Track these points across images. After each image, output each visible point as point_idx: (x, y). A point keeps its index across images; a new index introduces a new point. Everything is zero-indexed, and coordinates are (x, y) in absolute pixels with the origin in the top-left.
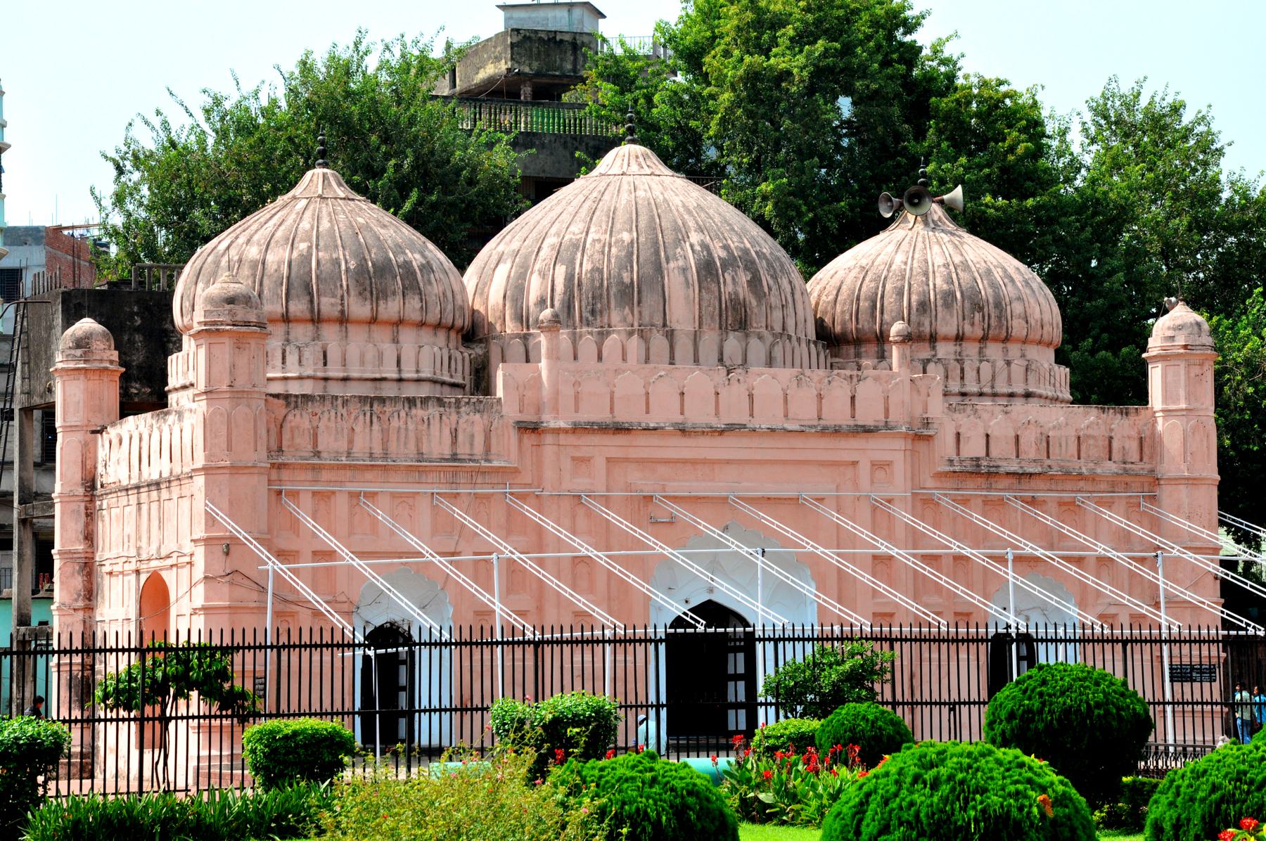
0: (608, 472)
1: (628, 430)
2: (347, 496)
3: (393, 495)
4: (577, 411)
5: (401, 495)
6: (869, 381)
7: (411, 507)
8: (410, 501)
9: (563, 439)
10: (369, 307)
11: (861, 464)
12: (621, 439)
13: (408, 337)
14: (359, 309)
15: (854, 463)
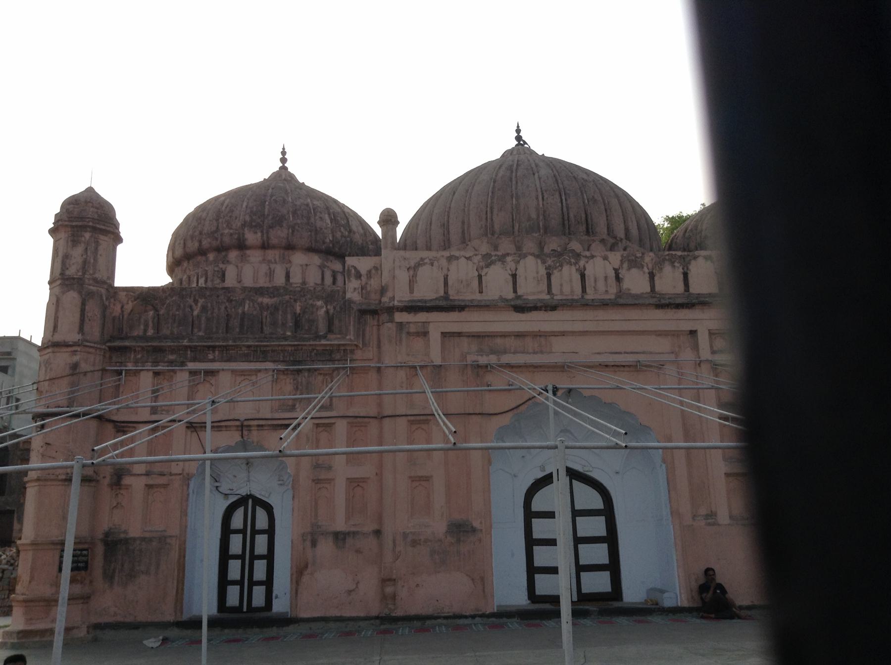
0: (443, 343)
1: (461, 308)
2: (186, 375)
3: (233, 371)
4: (411, 291)
5: (242, 373)
6: (701, 261)
7: (254, 384)
8: (253, 378)
9: (399, 317)
10: (259, 234)
11: (699, 334)
12: (454, 316)
13: (299, 258)
14: (252, 238)
15: (693, 333)
